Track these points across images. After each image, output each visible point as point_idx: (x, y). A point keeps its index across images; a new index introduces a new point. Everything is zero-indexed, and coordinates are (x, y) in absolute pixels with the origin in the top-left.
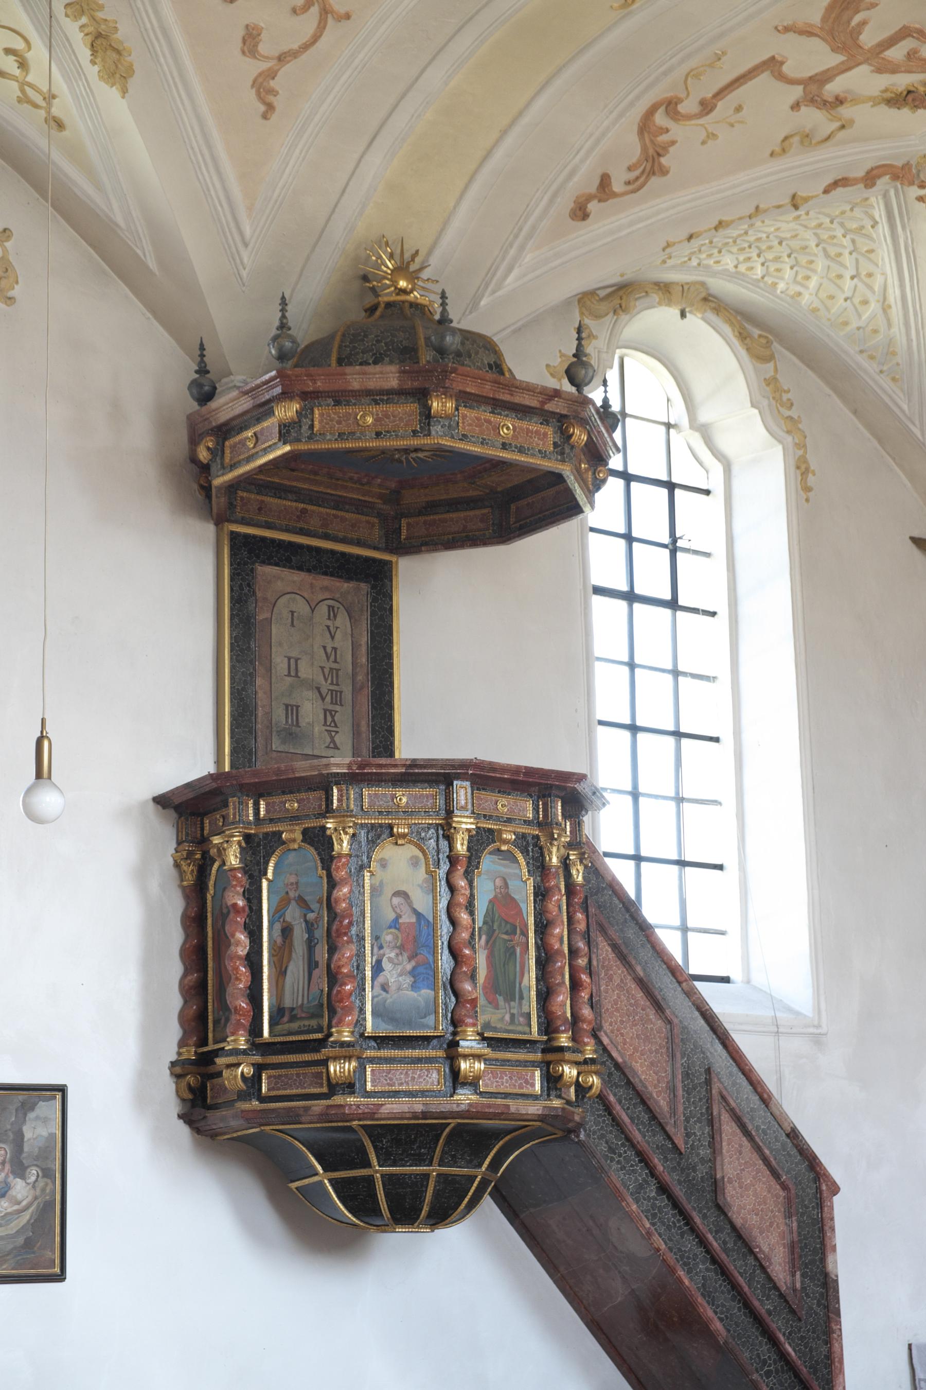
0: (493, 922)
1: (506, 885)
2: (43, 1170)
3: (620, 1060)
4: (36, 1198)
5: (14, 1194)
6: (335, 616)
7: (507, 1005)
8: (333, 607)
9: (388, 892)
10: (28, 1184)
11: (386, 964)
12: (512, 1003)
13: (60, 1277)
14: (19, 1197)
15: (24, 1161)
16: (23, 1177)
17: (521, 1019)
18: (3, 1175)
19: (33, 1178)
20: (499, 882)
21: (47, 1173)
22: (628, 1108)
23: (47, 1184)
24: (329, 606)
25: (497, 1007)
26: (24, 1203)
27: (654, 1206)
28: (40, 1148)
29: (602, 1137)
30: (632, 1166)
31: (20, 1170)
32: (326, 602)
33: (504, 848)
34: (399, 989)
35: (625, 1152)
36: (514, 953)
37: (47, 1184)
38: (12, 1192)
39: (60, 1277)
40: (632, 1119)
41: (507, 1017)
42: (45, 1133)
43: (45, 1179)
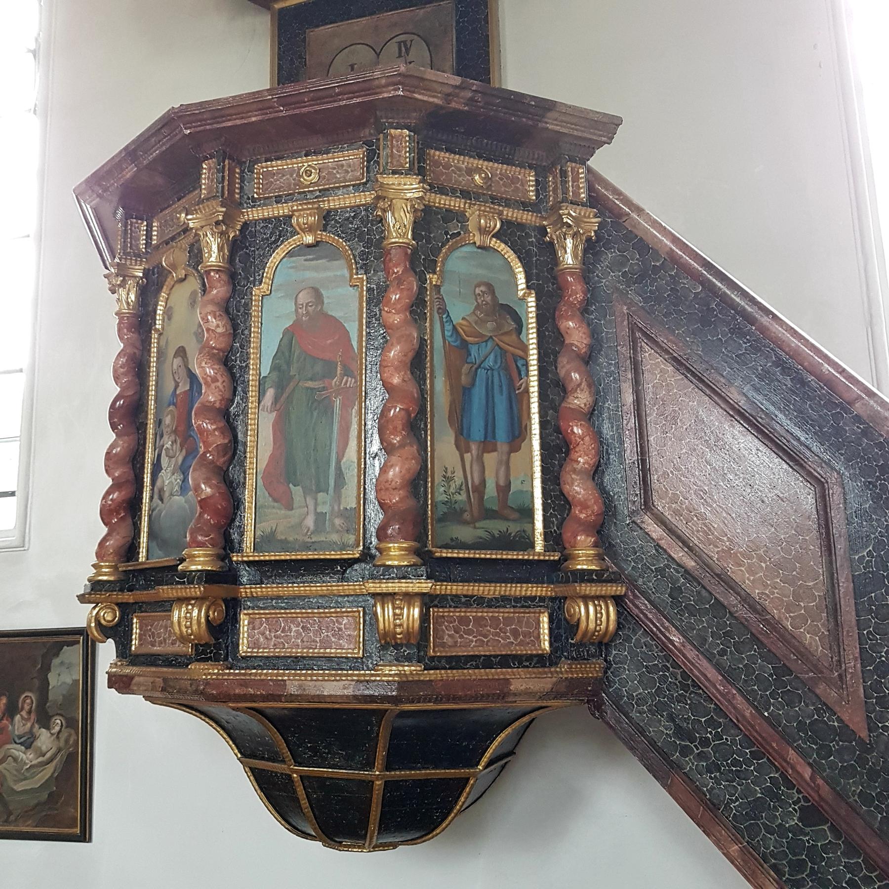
0: (289, 363)
1: (318, 296)
2: (67, 720)
3: (690, 563)
4: (59, 750)
5: (39, 745)
6: (407, 51)
7: (310, 502)
8: (405, 42)
9: (171, 352)
10: (52, 734)
11: (164, 461)
12: (321, 495)
13: (84, 836)
14: (44, 748)
15: (49, 710)
16: (48, 728)
17: (338, 522)
18: (29, 725)
19: (57, 728)
20: (303, 298)
21: (70, 723)
22: (723, 653)
23: (70, 735)
24: (400, 43)
25: (290, 507)
26: (48, 755)
27: (795, 846)
28: (64, 696)
29: (657, 709)
30: (735, 763)
31: (44, 720)
32: (395, 40)
33: (309, 239)
34: (172, 495)
35: (718, 736)
36: (328, 410)
37: (70, 735)
38: (38, 743)
39: (84, 836)
40: (729, 675)
41: (310, 522)
42: (69, 681)
43: (69, 730)
